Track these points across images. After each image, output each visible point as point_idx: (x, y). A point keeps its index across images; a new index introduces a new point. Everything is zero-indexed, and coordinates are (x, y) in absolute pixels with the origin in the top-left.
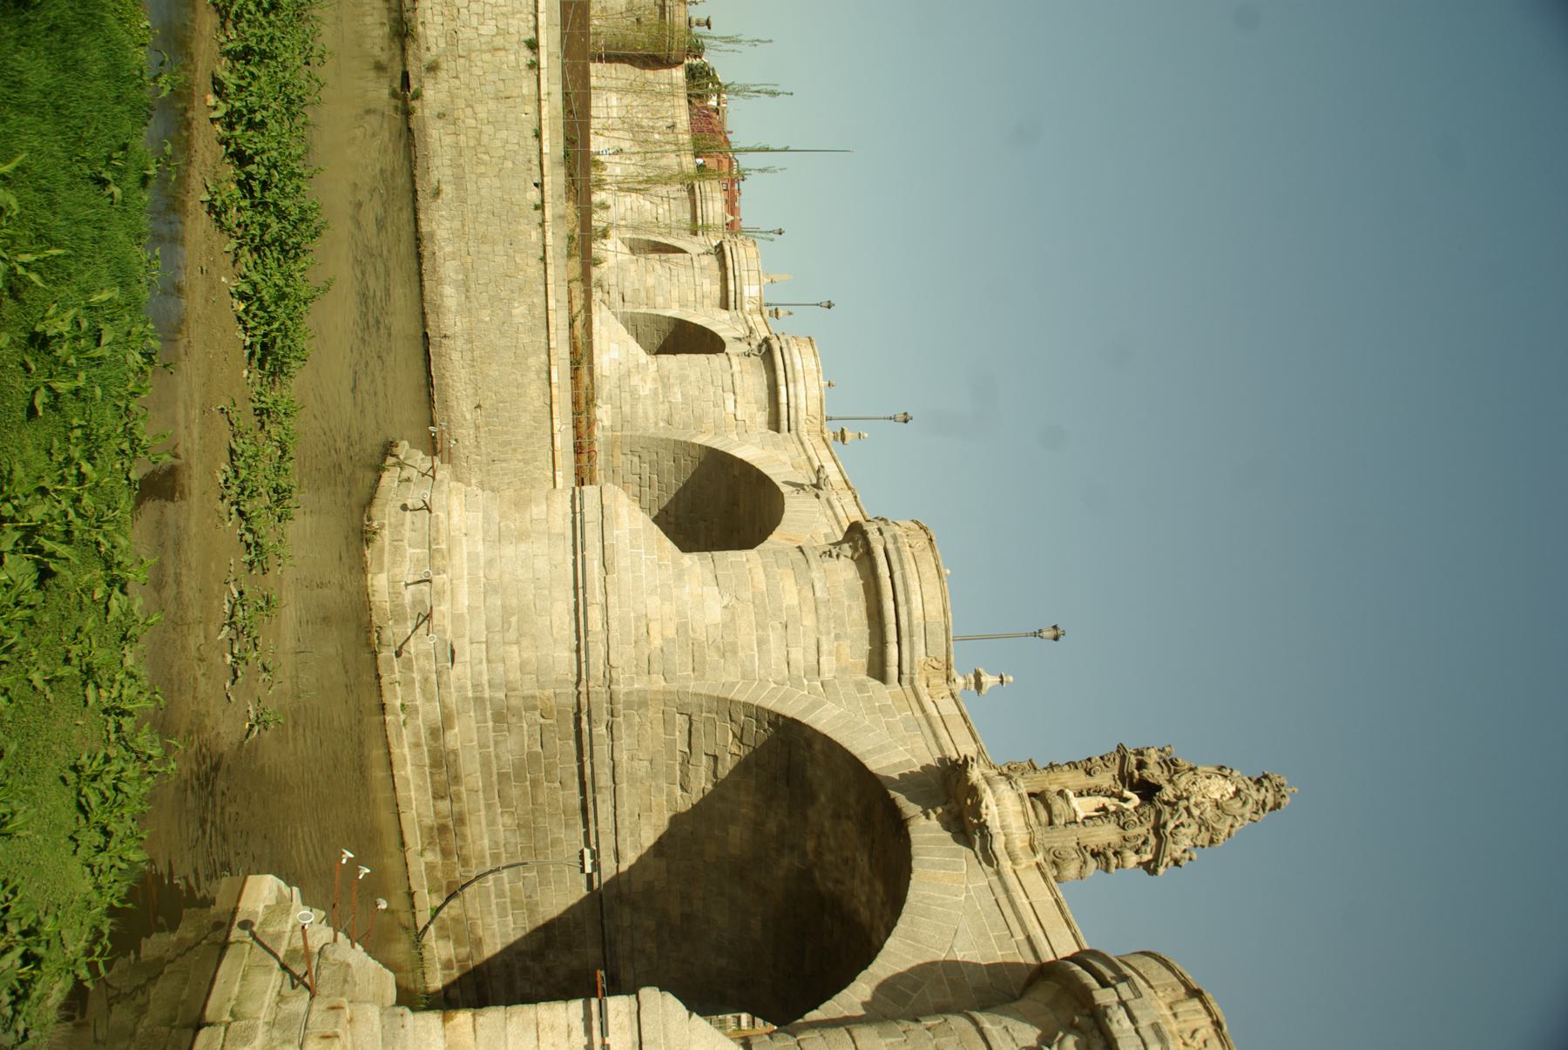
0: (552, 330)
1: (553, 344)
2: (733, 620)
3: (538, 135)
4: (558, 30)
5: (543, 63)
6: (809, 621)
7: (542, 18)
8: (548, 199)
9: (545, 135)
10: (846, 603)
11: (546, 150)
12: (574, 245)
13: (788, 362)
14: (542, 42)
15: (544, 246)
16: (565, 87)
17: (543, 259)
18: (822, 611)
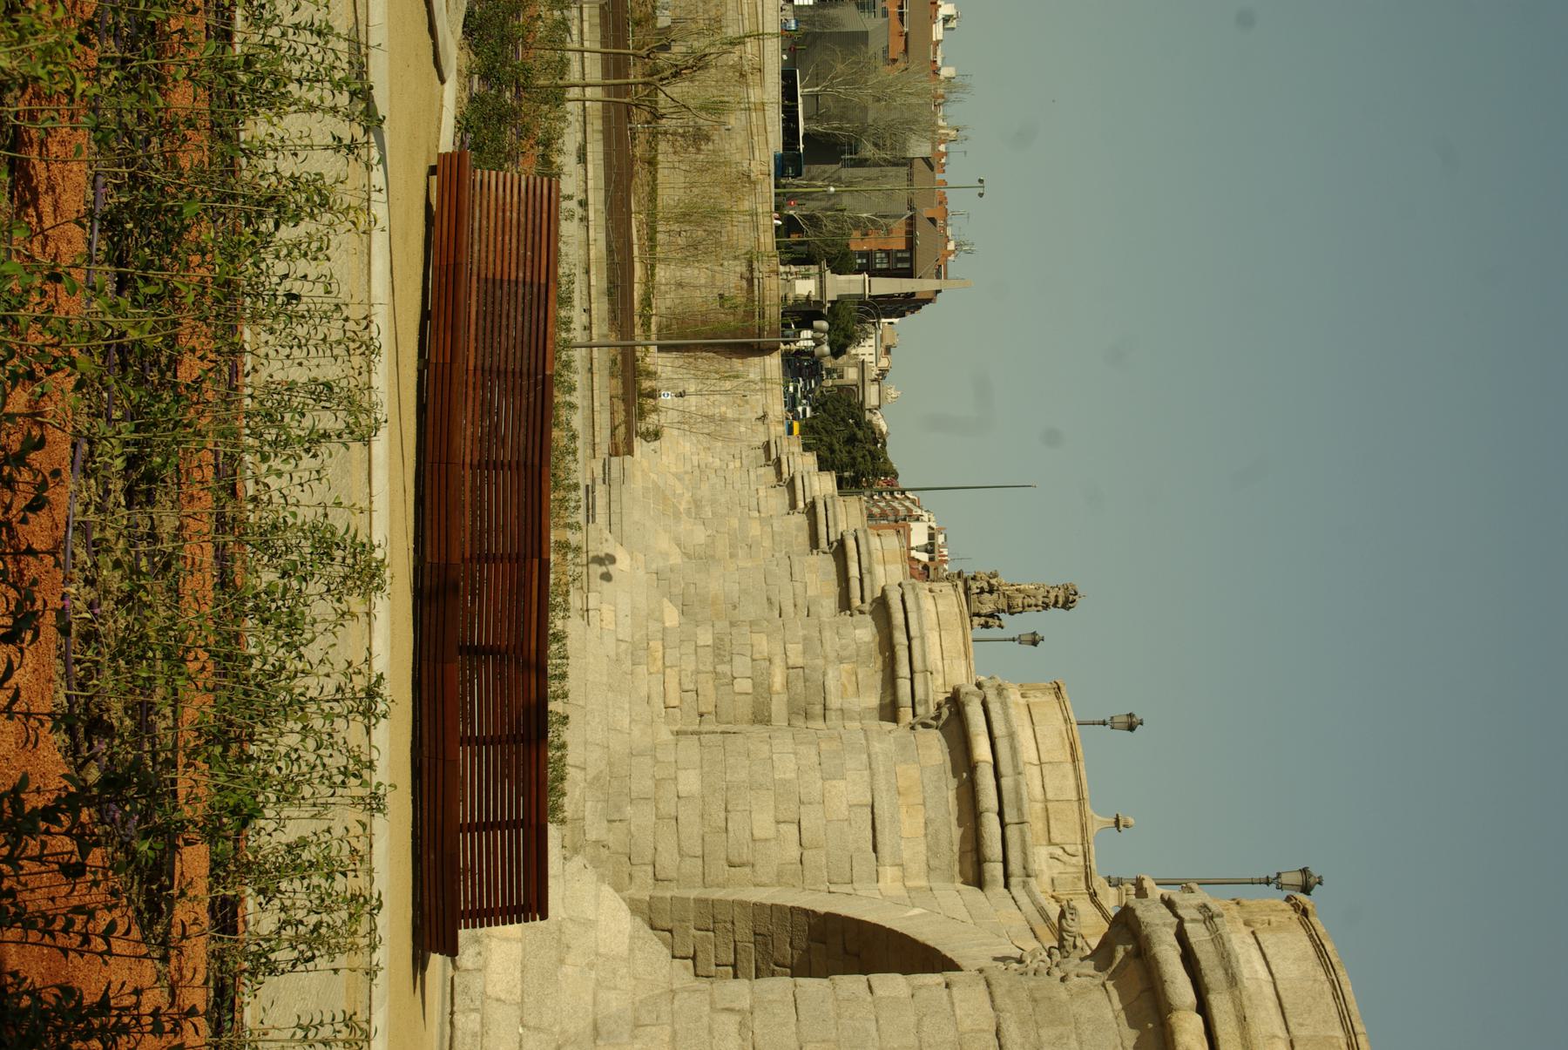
0: (597, 428)
1: (597, 440)
2: (713, 543)
3: (588, 272)
4: (602, 193)
5: (591, 216)
6: (767, 543)
7: (590, 183)
8: (594, 321)
9: (593, 271)
10: (795, 533)
11: (593, 282)
12: (615, 369)
13: (806, 483)
14: (591, 201)
15: (591, 359)
16: (608, 235)
17: (591, 370)
18: (777, 538)
